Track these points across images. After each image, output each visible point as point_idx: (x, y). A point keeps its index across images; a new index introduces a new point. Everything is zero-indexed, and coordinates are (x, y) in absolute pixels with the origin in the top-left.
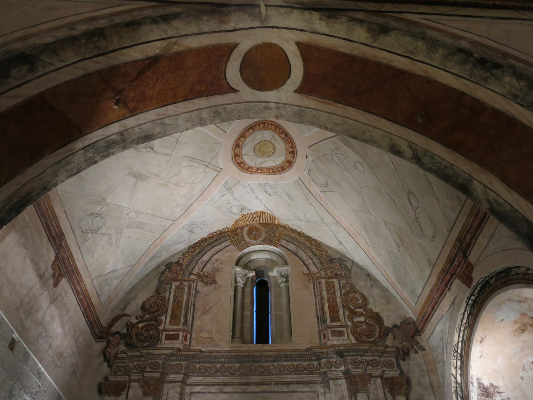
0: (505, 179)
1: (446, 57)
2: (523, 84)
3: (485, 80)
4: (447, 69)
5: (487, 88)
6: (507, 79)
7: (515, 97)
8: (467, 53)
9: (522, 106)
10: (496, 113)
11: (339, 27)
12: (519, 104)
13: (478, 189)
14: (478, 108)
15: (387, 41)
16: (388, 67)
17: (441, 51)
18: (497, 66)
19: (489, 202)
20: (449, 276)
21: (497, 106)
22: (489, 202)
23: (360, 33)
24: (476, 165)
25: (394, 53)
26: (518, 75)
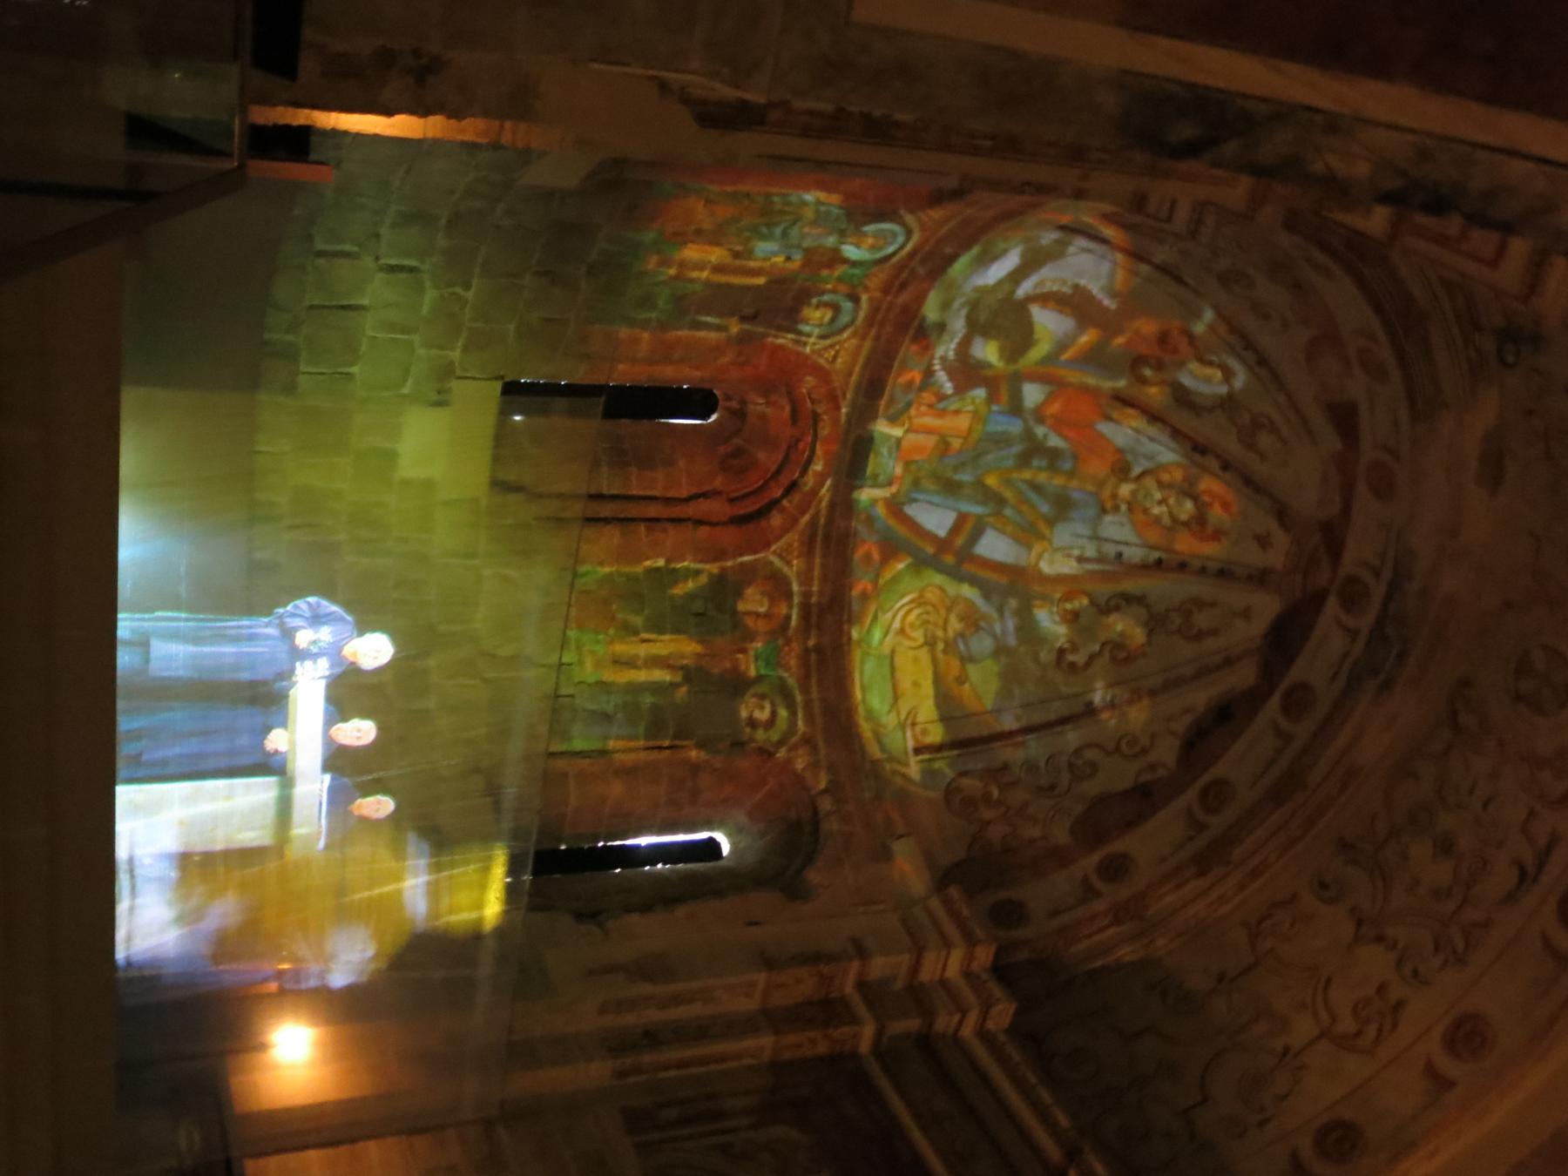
2: (1318, 167)
4: (1547, 168)
5: (1411, 131)
6: (1362, 169)
7: (1333, 124)
9: (1309, 108)
10: (1378, 66)
12: (1317, 111)
21: (1377, 87)
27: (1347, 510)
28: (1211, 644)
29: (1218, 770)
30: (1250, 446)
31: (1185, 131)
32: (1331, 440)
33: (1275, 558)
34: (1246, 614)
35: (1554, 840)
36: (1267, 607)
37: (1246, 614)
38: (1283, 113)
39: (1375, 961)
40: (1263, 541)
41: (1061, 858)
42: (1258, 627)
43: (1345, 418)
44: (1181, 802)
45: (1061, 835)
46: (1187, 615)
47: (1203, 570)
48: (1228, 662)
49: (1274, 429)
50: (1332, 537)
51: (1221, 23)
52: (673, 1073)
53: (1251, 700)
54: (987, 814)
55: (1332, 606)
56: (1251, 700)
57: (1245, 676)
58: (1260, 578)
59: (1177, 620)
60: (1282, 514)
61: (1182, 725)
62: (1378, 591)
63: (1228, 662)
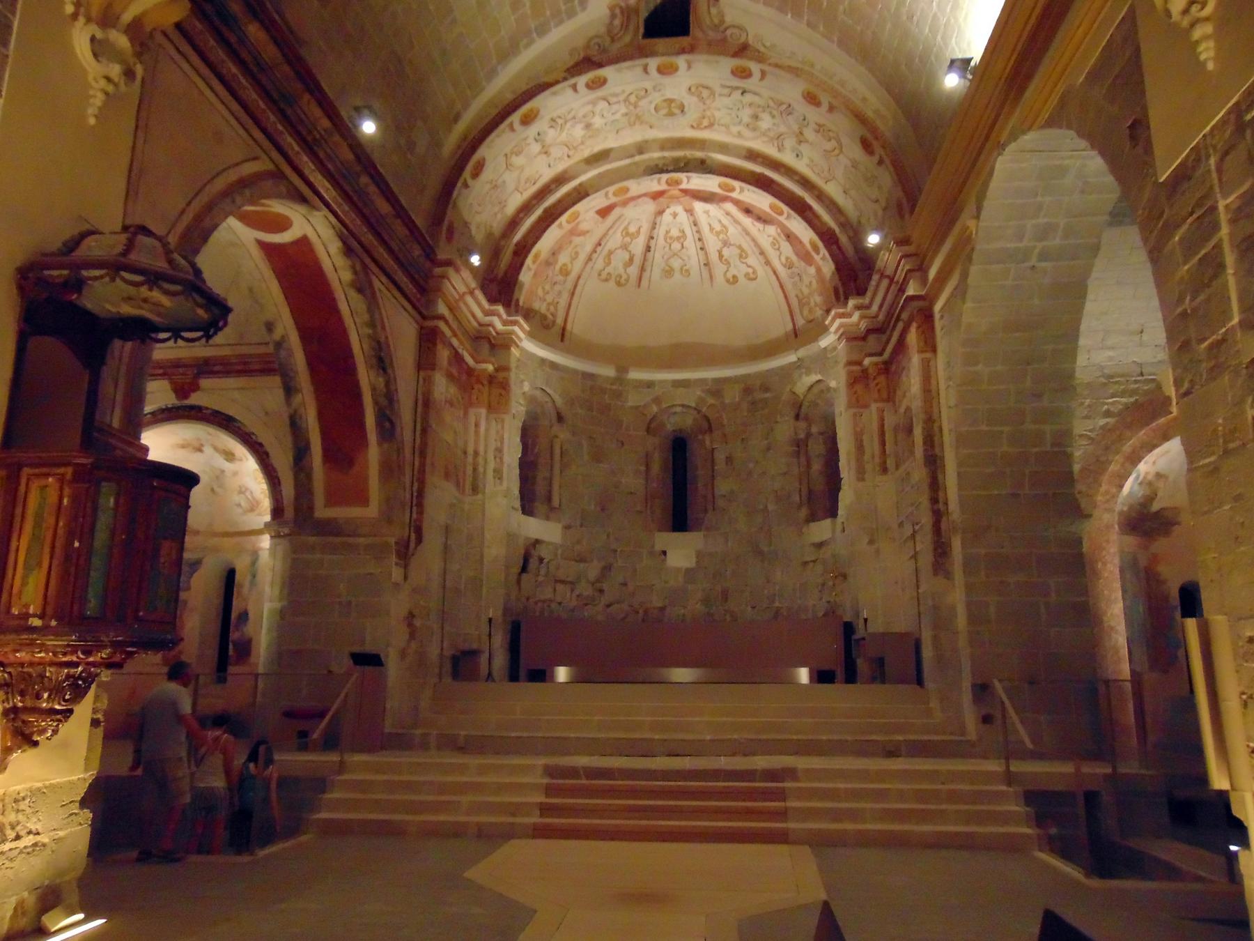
0: (321, 415)
1: (369, 336)
3: (372, 367)
6: (381, 379)
7: (374, 389)
8: (380, 349)
11: (341, 261)
13: (297, 399)
14: (351, 370)
15: (353, 294)
16: (334, 299)
17: (371, 331)
18: (384, 370)
19: (295, 411)
20: (161, 371)
22: (295, 411)
23: (347, 276)
24: (312, 389)
25: (349, 305)
26: (387, 384)
27: (645, 195)
28: (725, 221)
29: (768, 210)
30: (638, 232)
31: (387, 424)
32: (616, 212)
33: (679, 209)
34: (707, 212)
35: (723, 86)
36: (699, 206)
37: (707, 212)
38: (376, 403)
39: (809, 134)
40: (675, 215)
41: (819, 270)
42: (708, 206)
43: (604, 212)
44: (785, 222)
45: (812, 270)
46: (718, 234)
47: (698, 232)
48: (728, 214)
49: (626, 228)
50: (657, 196)
51: (361, 426)
52: (887, 447)
53: (737, 203)
54: (812, 304)
55: (684, 186)
56: (737, 203)
57: (729, 206)
58: (690, 211)
59: (721, 236)
60: (661, 213)
61: (760, 226)
62: (665, 177)
63: (728, 214)
